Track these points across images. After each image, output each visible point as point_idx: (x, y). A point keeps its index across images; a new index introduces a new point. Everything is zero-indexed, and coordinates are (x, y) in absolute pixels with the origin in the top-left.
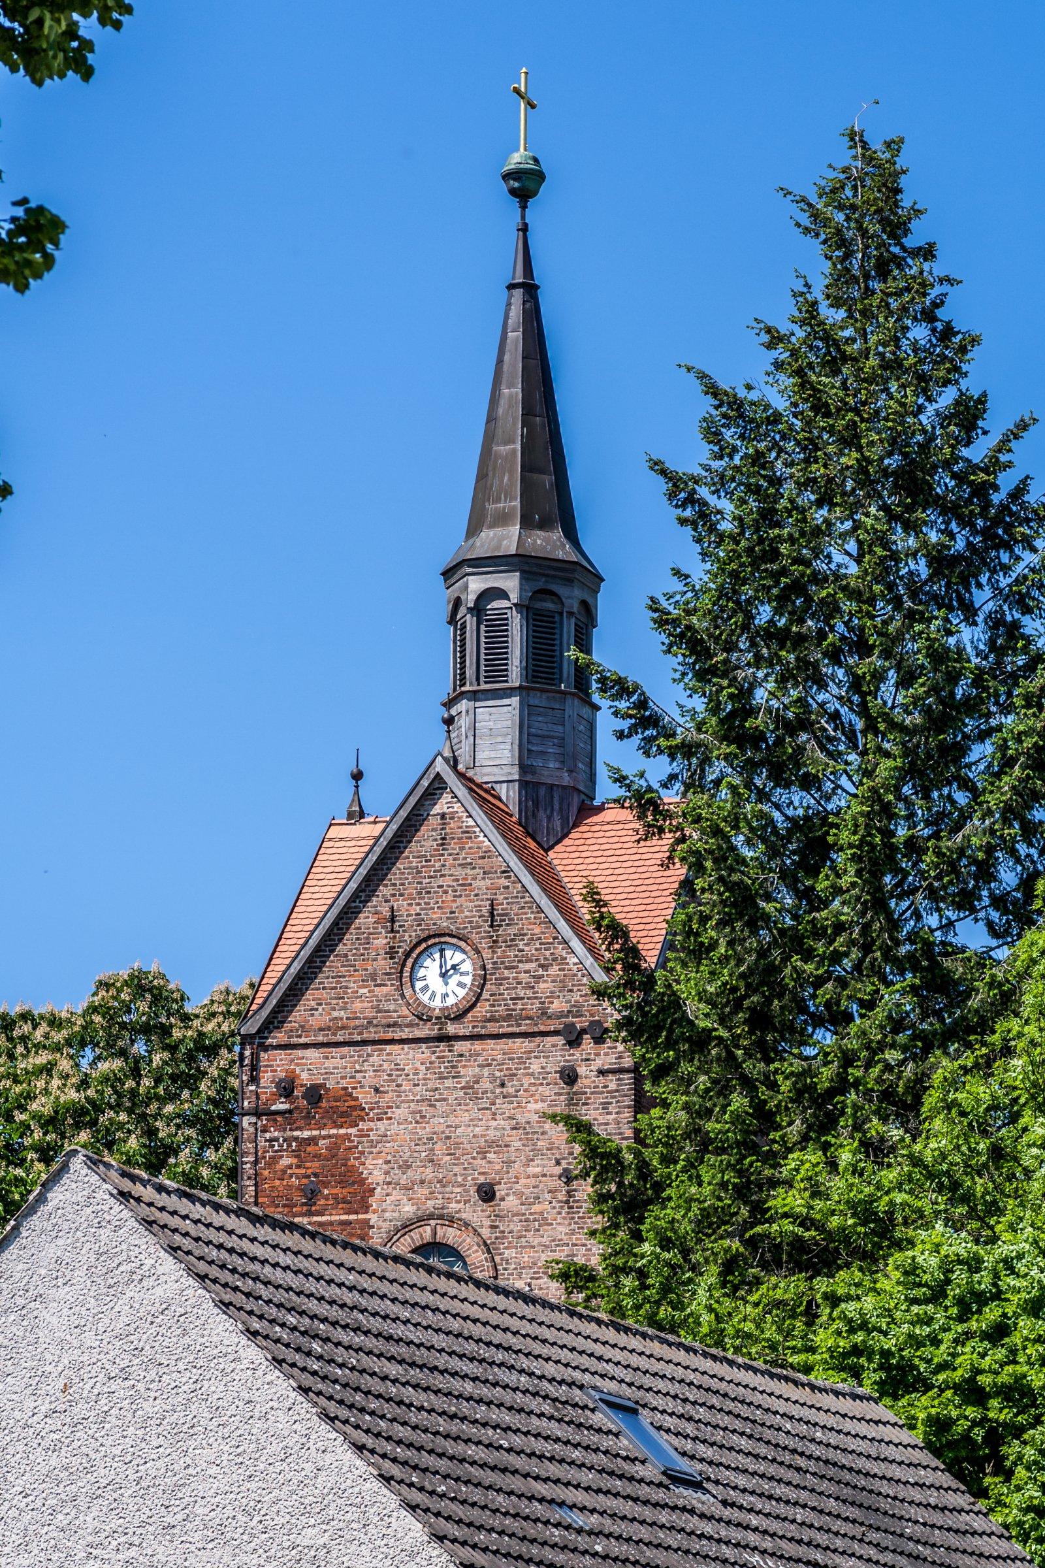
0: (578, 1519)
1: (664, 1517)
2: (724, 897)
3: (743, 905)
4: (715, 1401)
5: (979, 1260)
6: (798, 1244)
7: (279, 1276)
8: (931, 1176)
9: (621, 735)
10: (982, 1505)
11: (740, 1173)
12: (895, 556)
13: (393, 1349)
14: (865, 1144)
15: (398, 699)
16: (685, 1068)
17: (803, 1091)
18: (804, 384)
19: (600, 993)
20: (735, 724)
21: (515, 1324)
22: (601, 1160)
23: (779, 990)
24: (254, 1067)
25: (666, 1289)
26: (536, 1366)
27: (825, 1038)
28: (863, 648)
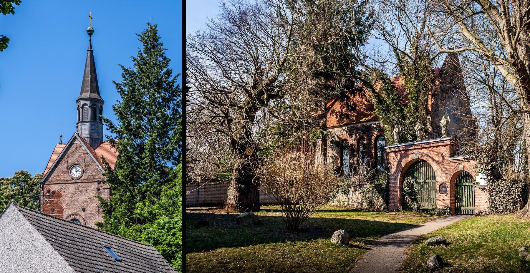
0: (100, 267)
1: (115, 267)
2: (126, 157)
3: (129, 159)
4: (124, 246)
5: (171, 222)
6: (139, 219)
7: (47, 224)
8: (162, 207)
9: (107, 129)
10: (171, 265)
11: (129, 206)
12: (156, 98)
13: (67, 237)
14: (151, 201)
15: (67, 122)
16: (119, 188)
17: (140, 192)
18: (140, 68)
19: (104, 175)
20: (128, 127)
21: (89, 233)
22: (104, 204)
23: (135, 174)
24: (43, 188)
25: (115, 227)
26: (93, 240)
27: (143, 183)
28: (150, 114)
